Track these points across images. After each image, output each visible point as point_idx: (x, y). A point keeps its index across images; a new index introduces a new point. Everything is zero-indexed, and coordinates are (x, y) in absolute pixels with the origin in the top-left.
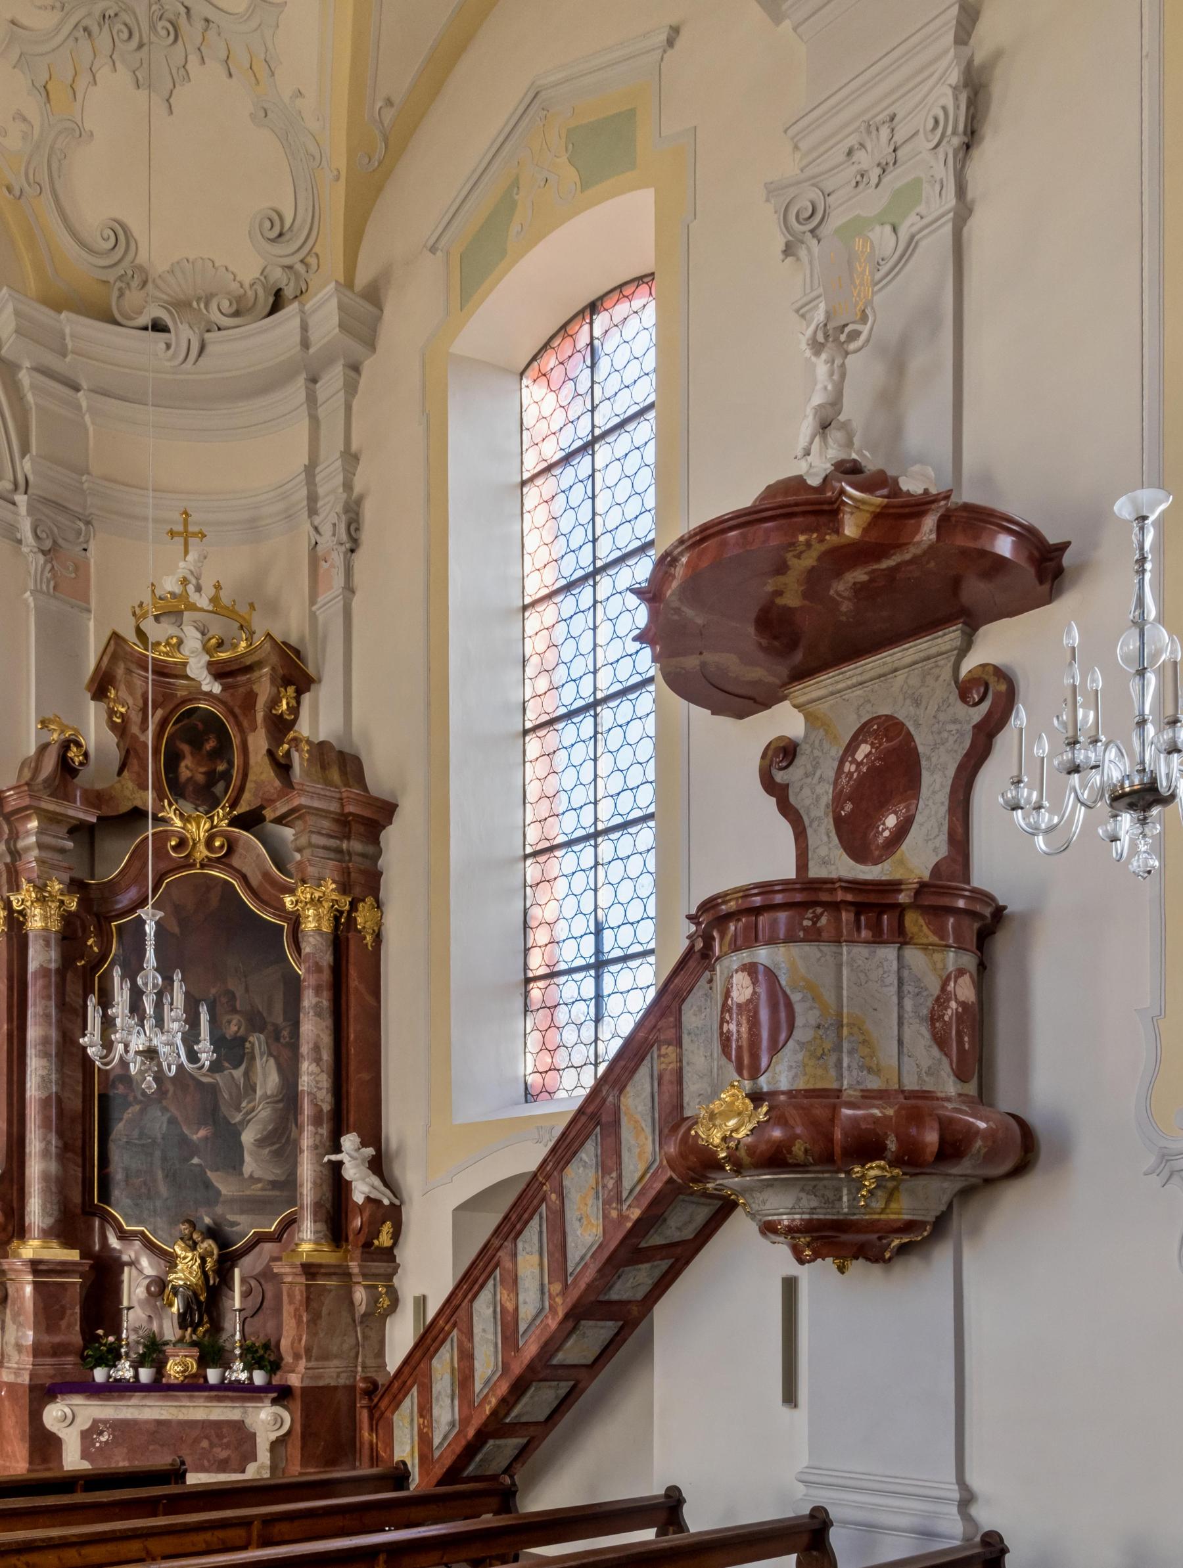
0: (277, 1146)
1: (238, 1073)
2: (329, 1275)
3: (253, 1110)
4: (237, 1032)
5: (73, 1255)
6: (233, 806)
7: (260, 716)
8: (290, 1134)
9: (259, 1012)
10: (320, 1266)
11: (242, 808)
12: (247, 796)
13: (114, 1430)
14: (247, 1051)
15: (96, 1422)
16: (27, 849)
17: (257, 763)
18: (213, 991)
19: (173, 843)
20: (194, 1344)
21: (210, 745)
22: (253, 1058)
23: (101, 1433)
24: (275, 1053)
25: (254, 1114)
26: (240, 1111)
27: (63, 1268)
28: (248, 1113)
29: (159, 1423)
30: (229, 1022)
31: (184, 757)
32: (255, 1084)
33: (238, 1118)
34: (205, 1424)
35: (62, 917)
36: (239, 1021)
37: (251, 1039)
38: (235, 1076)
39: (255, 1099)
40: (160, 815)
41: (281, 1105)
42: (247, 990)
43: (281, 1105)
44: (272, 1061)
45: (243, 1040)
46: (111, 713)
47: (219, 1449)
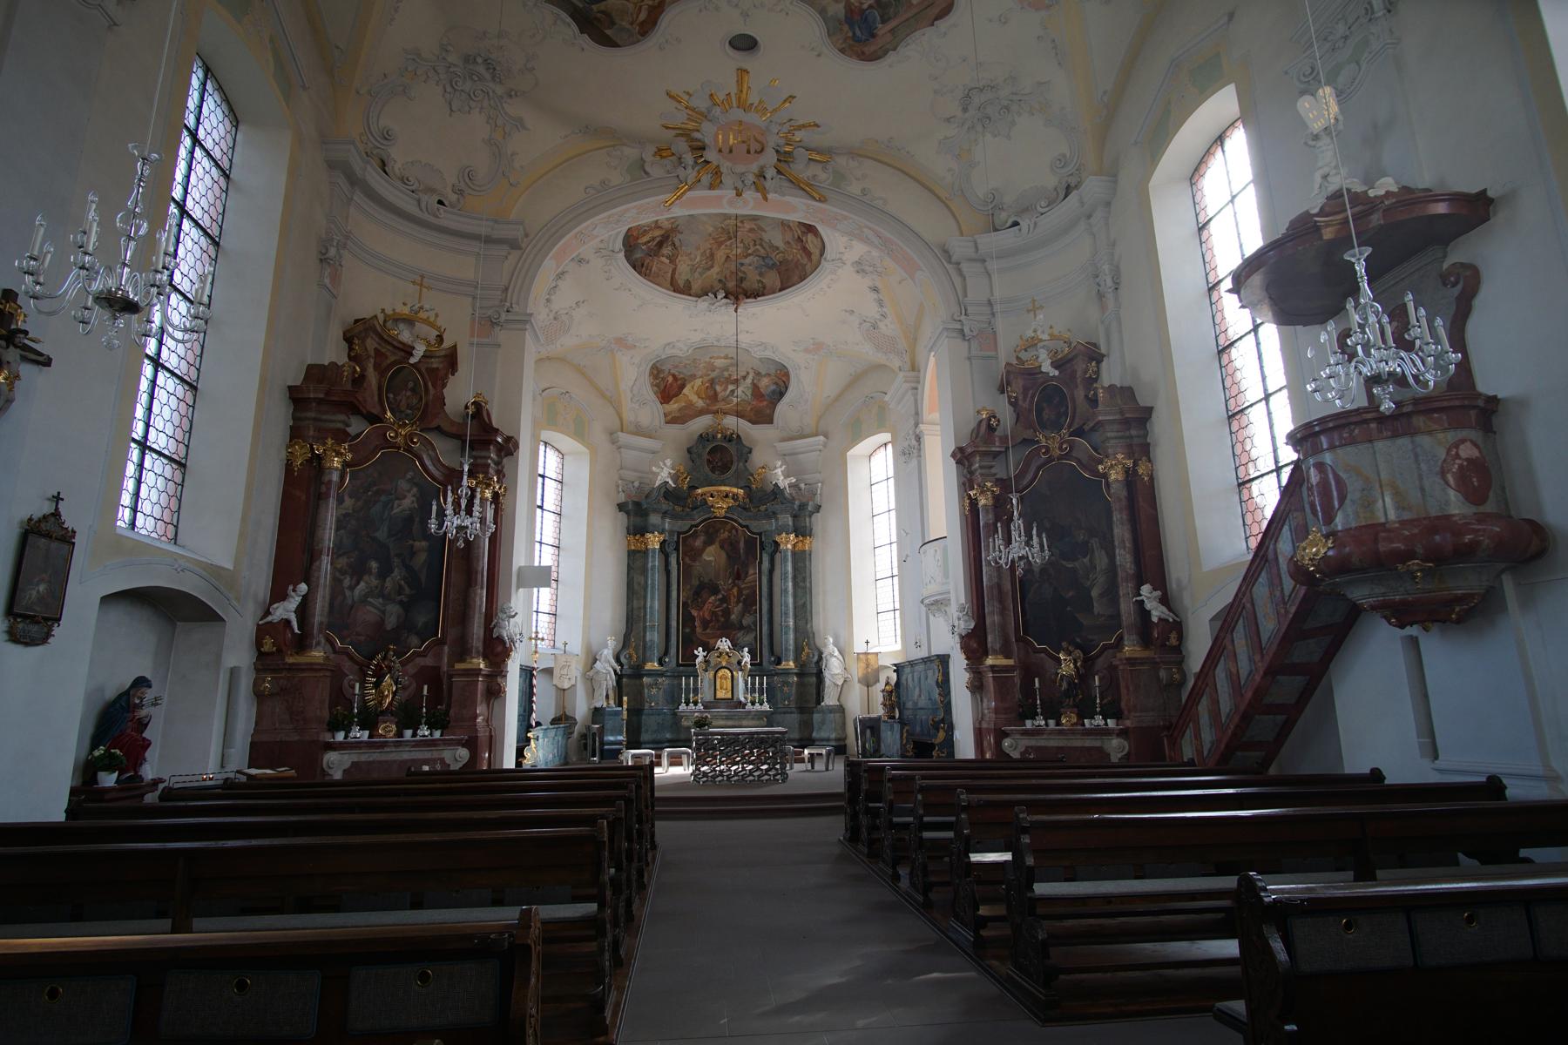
1: (1086, 560)
2: (1142, 664)
3: (1096, 578)
5: (1011, 662)
10: (1136, 659)
15: (1027, 747)
16: (976, 470)
20: (1075, 706)
22: (1093, 551)
23: (1030, 754)
27: (1006, 669)
29: (1058, 748)
33: (1089, 583)
34: (1082, 749)
35: (994, 498)
44: (1103, 552)
46: (1009, 397)
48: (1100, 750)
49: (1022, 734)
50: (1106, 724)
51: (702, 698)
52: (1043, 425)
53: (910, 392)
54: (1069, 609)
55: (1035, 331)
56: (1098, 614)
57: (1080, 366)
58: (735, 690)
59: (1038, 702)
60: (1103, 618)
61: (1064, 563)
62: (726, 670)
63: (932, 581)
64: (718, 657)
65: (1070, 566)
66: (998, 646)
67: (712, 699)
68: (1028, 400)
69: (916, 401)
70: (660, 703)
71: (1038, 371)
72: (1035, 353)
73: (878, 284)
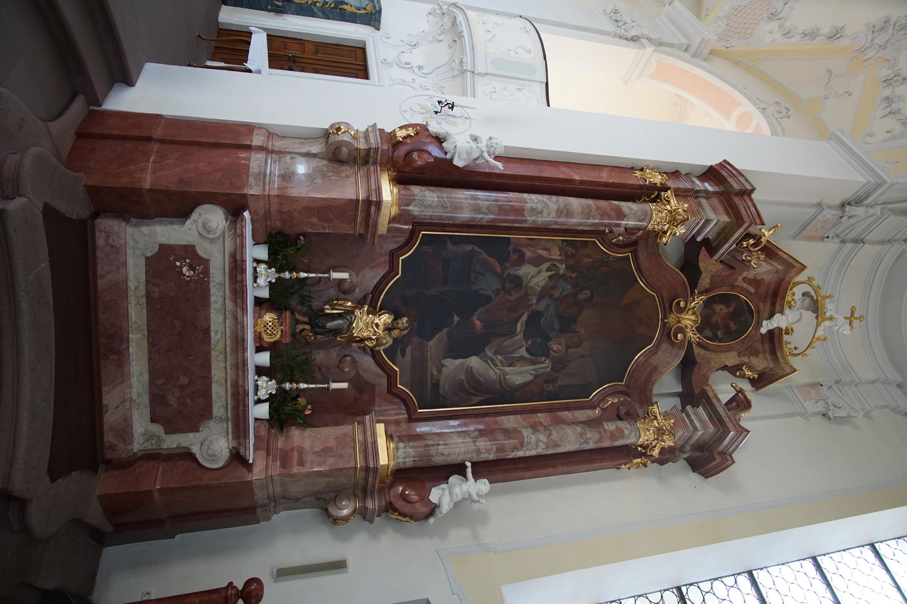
0: (467, 385)
1: (523, 352)
3: (495, 365)
4: (553, 350)
6: (699, 344)
7: (746, 359)
8: (477, 396)
9: (566, 366)
11: (696, 350)
12: (703, 352)
13: (196, 281)
14: (539, 358)
15: (206, 262)
17: (721, 358)
18: (582, 331)
19: (681, 303)
21: (733, 326)
22: (534, 363)
23: (191, 267)
24: (536, 380)
25: (492, 366)
26: (494, 355)
28: (492, 360)
29: (207, 331)
30: (560, 344)
31: (727, 307)
32: (514, 366)
36: (561, 351)
37: (547, 361)
38: (520, 350)
39: (503, 367)
40: (696, 290)
41: (498, 387)
42: (582, 356)
43: (498, 387)
44: (531, 378)
45: (547, 356)
47: (178, 395)
48: (206, 414)
49: (233, 256)
50: (259, 401)
52: (707, 304)
53: (685, 41)
54: (456, 318)
55: (831, 318)
56: (443, 365)
57: (761, 363)
59: (303, 275)
60: (435, 373)
61: (525, 318)
63: (489, 36)
65: (519, 325)
66: (414, 209)
68: (745, 285)
69: (672, 46)
71: (778, 307)
72: (797, 307)
73: (844, 42)
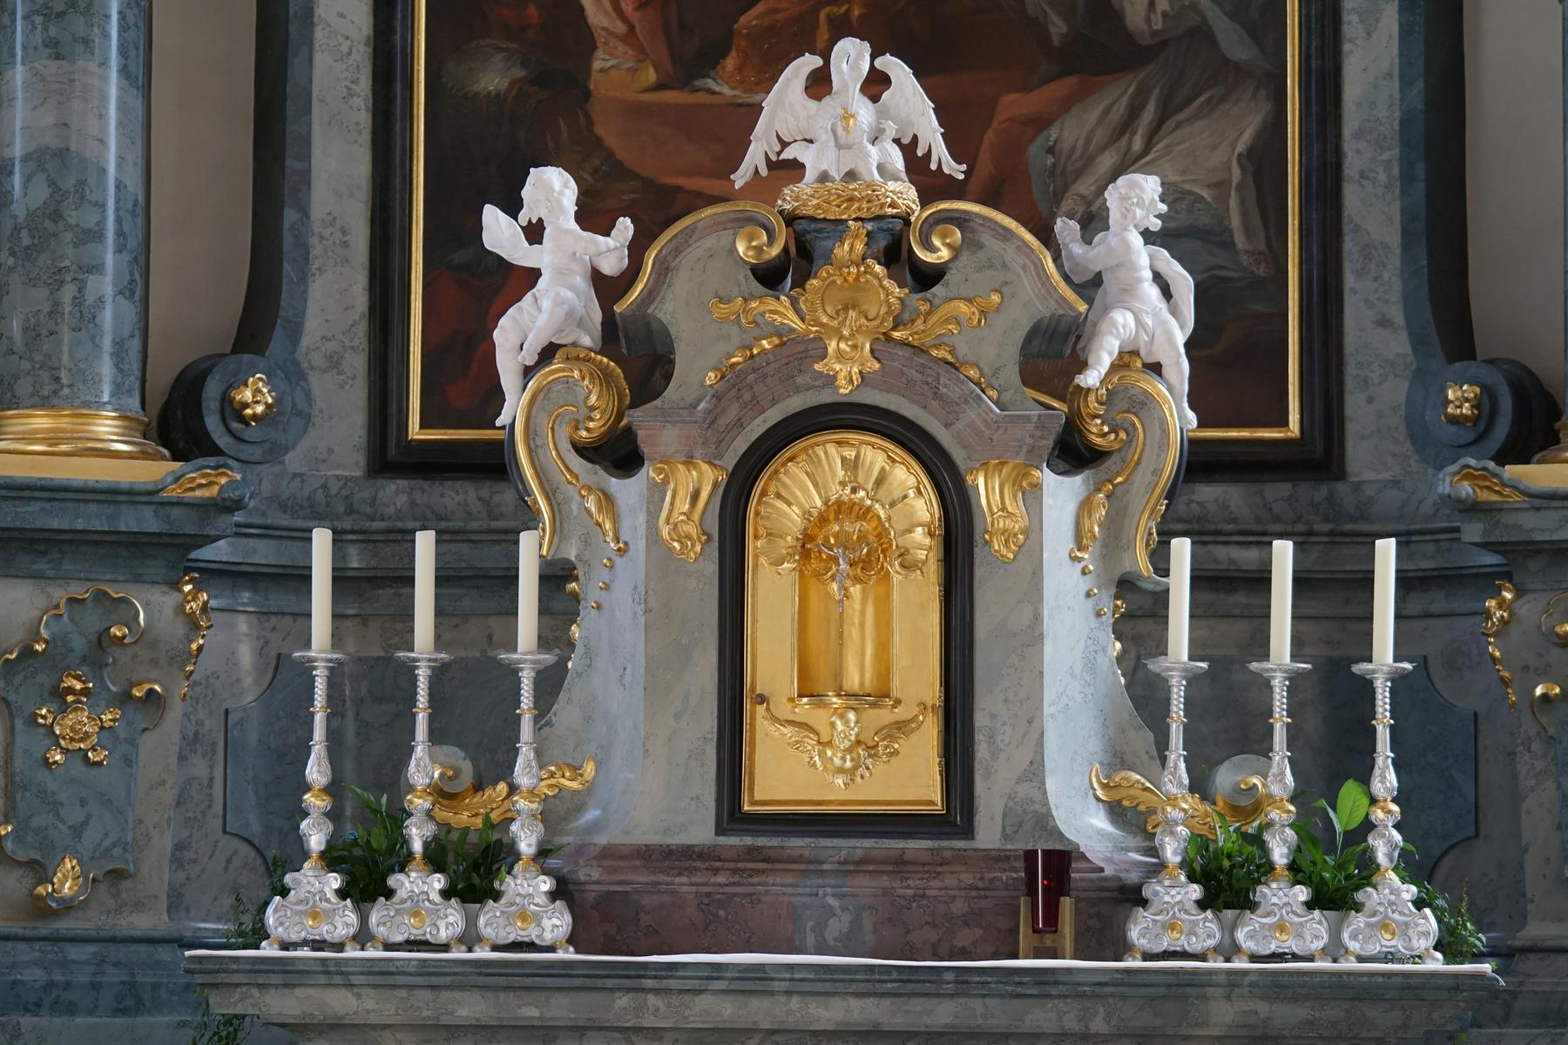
51: (553, 815)
58: (987, 709)
62: (875, 454)
64: (769, 276)
67: (700, 830)
70: (155, 875)
